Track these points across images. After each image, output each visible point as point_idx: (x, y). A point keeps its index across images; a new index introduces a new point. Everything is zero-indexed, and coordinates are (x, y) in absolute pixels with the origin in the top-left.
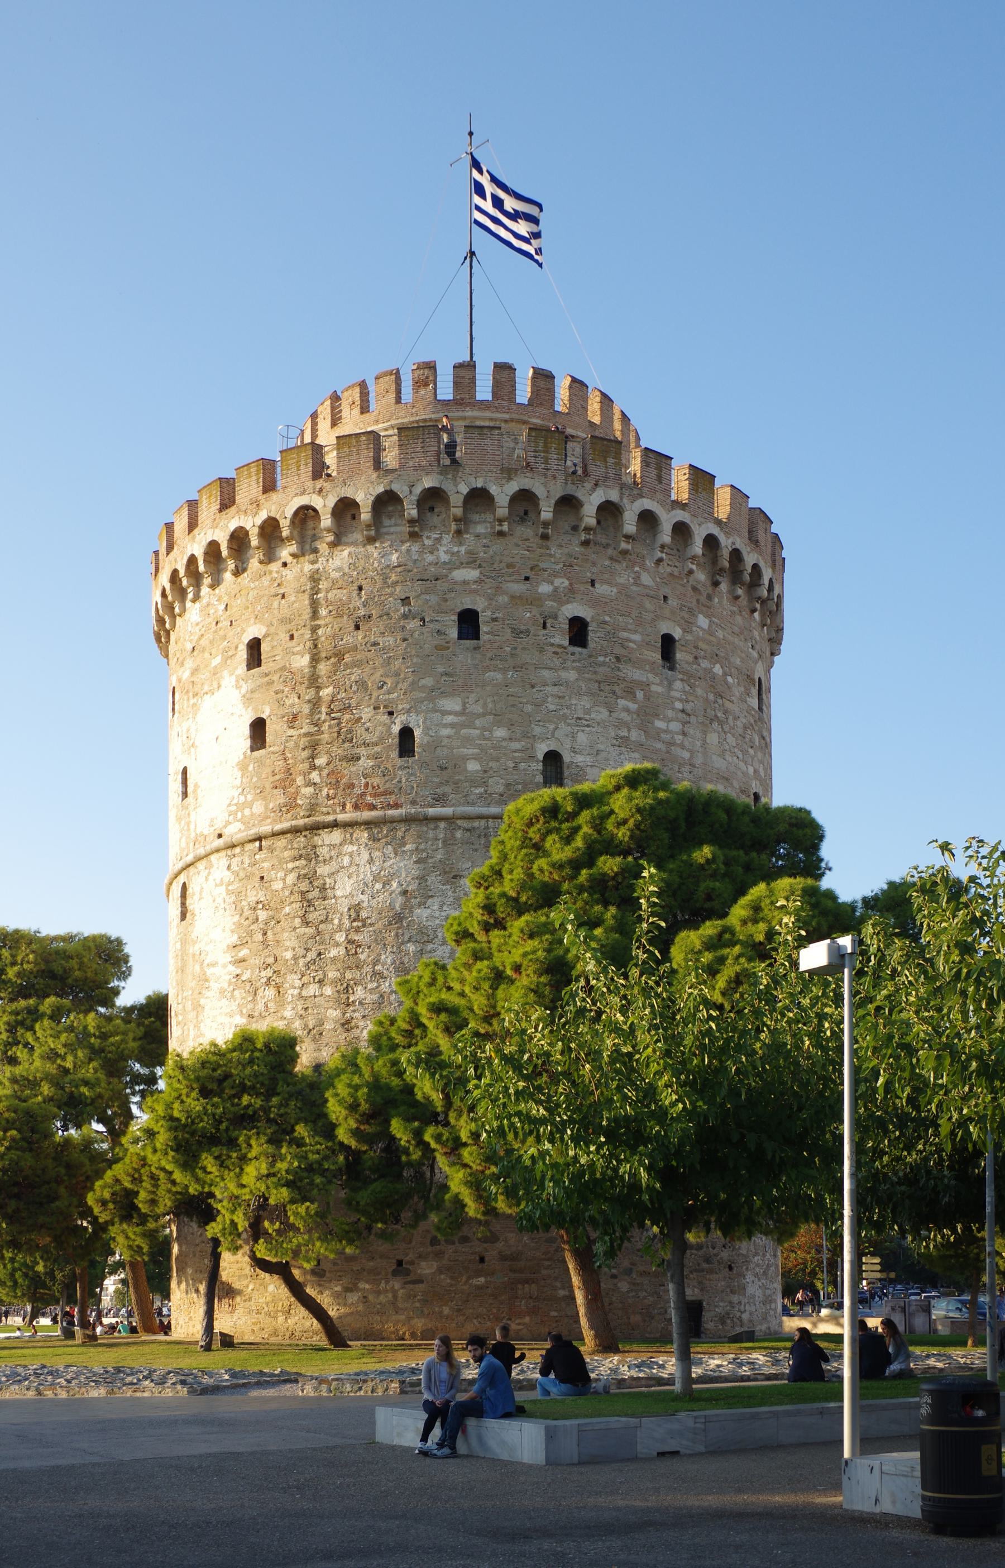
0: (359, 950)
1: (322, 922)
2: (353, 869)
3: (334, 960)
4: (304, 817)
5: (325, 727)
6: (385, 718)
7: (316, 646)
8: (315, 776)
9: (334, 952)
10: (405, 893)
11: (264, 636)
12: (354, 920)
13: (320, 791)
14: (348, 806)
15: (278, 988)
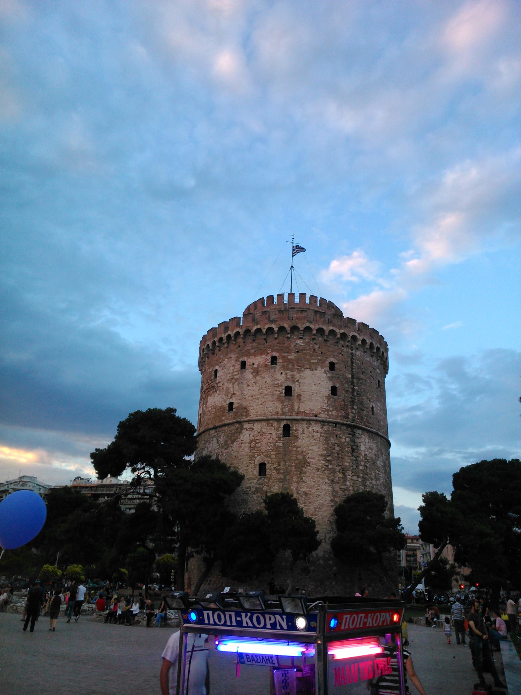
0: (367, 469)
1: (357, 457)
2: (364, 443)
3: (361, 469)
4: (351, 422)
5: (356, 398)
6: (369, 402)
7: (353, 373)
8: (353, 410)
9: (361, 468)
10: (375, 454)
11: (337, 363)
12: (365, 459)
13: (355, 416)
14: (362, 423)
15: (344, 474)
